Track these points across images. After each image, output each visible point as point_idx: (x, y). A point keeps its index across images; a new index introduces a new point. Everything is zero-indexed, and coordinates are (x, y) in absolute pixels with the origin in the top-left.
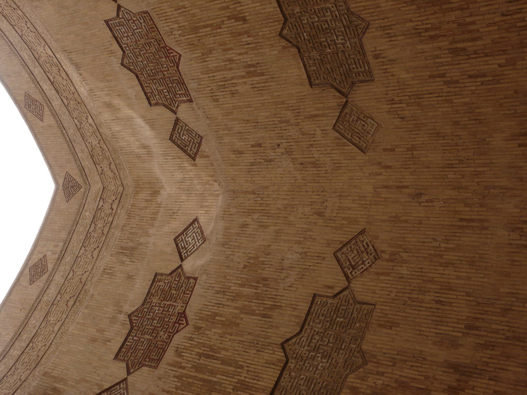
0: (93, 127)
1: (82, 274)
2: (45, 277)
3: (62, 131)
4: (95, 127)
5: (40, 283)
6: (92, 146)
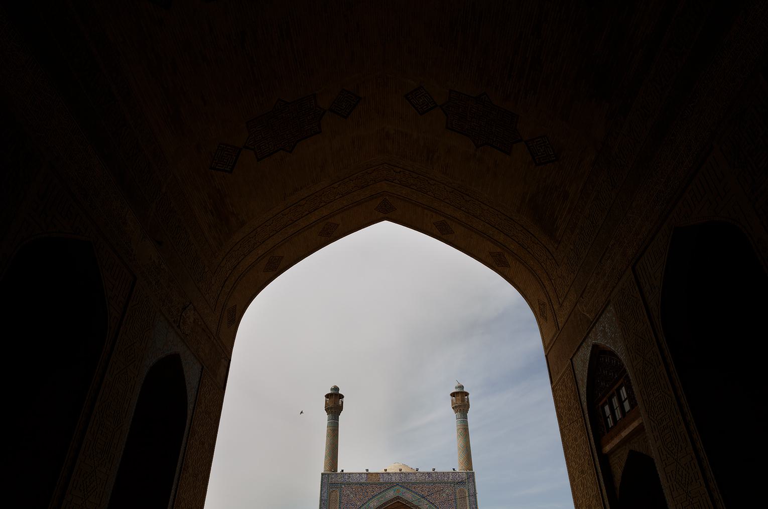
0: (340, 184)
1: (447, 191)
3: (345, 210)
4: (340, 182)
6: (355, 187)
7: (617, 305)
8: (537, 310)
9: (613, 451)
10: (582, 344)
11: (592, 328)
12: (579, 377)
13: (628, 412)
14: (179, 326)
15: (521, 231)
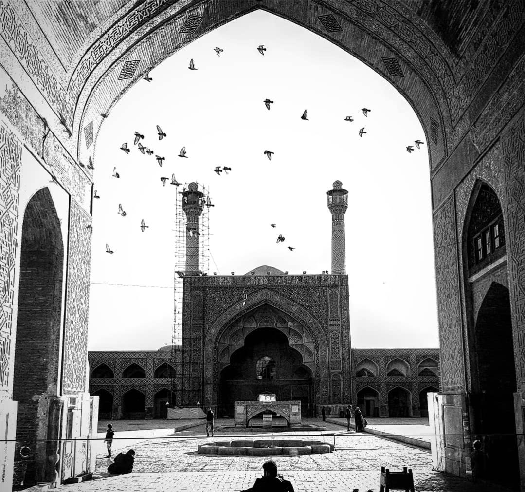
2: (336, 17)
5: (342, 22)
7: (505, 144)
8: (428, 128)
9: (478, 281)
10: (466, 176)
11: (479, 162)
12: (459, 208)
13: (497, 248)
14: (43, 158)
15: (420, 37)
